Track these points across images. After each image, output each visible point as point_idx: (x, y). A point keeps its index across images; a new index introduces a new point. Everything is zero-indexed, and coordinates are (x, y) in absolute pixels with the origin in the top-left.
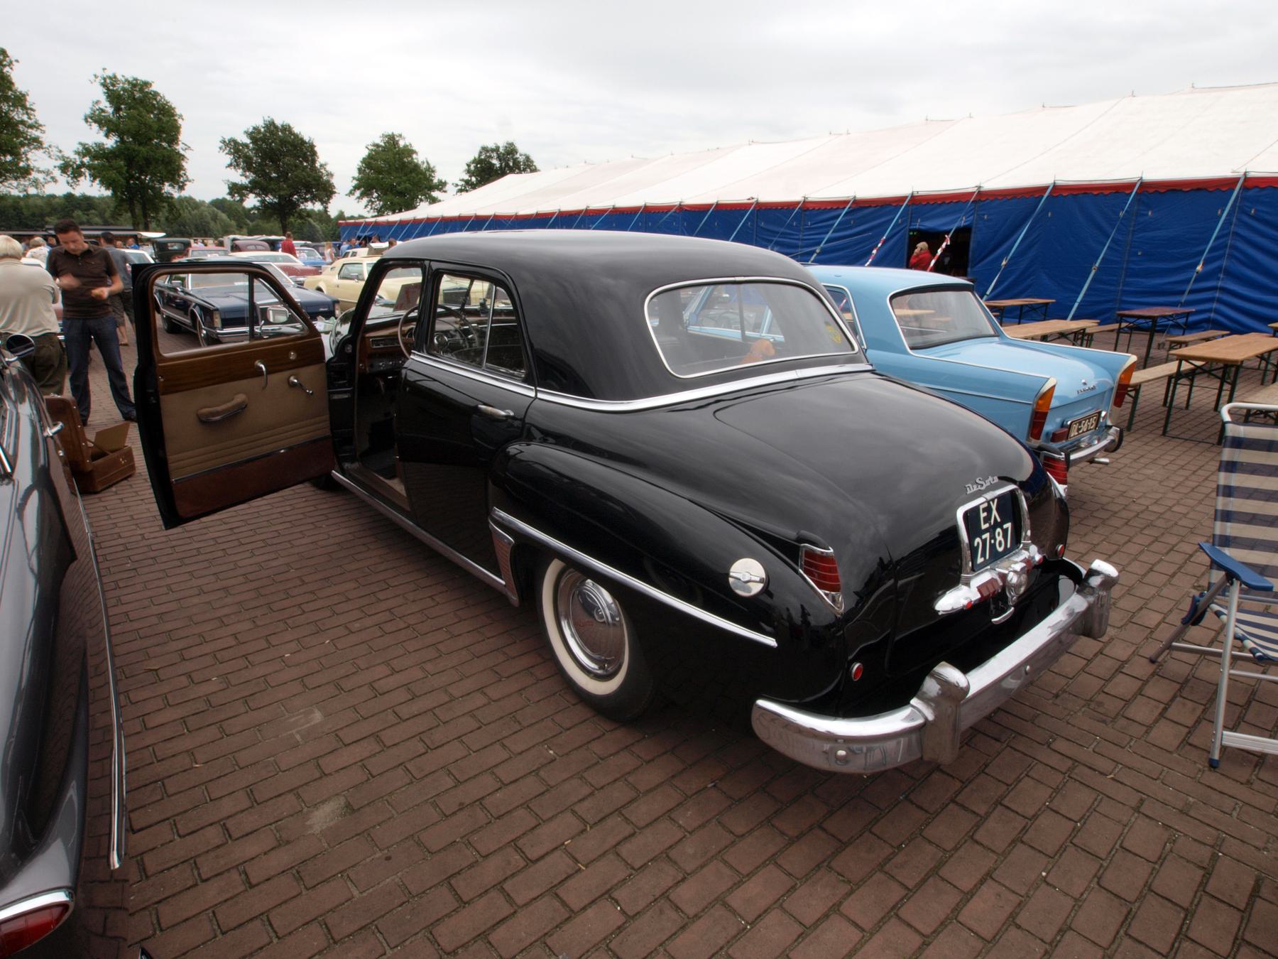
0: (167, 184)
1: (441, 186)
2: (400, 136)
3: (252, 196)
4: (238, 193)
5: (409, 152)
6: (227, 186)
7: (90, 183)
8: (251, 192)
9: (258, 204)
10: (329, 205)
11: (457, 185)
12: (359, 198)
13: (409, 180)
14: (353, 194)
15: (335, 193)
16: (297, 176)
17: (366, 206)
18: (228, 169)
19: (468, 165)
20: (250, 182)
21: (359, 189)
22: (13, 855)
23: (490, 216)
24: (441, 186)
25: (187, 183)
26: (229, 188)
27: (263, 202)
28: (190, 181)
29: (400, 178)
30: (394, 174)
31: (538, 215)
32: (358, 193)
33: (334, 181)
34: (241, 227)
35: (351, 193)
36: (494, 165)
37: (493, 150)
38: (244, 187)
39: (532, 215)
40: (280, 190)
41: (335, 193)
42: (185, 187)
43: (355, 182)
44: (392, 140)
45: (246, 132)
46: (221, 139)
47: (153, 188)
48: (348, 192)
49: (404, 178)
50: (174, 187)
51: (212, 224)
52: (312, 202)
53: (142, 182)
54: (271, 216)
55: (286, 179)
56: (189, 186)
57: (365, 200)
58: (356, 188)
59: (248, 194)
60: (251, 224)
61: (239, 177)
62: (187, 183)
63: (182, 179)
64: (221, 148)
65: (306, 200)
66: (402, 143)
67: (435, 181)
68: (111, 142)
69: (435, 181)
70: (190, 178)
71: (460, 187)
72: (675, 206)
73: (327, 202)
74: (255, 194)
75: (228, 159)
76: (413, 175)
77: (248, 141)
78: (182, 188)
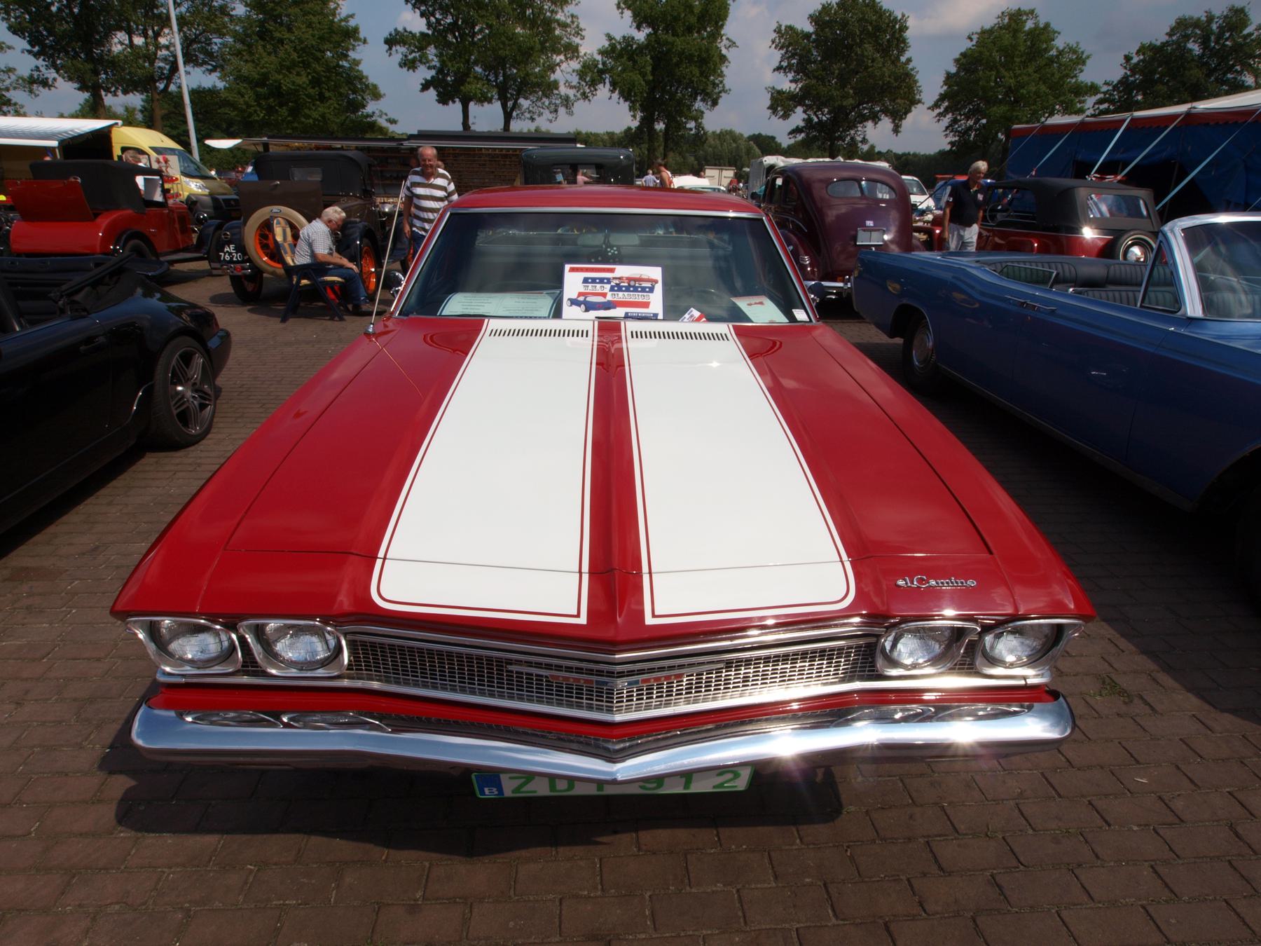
2: (1032, 12)
5: (1043, 34)
7: (609, 94)
12: (940, 115)
15: (919, 101)
17: (947, 128)
18: (776, 73)
19: (1128, 58)
26: (772, 98)
29: (1029, 75)
35: (936, 105)
36: (1191, 50)
37: (1196, 24)
41: (919, 101)
44: (1015, 19)
45: (811, 17)
46: (775, 26)
48: (931, 103)
58: (942, 98)
59: (796, 107)
61: (786, 84)
64: (773, 42)
66: (1029, 25)
68: (641, 36)
70: (727, 87)
73: (901, 119)
75: (776, 56)
77: (809, 28)
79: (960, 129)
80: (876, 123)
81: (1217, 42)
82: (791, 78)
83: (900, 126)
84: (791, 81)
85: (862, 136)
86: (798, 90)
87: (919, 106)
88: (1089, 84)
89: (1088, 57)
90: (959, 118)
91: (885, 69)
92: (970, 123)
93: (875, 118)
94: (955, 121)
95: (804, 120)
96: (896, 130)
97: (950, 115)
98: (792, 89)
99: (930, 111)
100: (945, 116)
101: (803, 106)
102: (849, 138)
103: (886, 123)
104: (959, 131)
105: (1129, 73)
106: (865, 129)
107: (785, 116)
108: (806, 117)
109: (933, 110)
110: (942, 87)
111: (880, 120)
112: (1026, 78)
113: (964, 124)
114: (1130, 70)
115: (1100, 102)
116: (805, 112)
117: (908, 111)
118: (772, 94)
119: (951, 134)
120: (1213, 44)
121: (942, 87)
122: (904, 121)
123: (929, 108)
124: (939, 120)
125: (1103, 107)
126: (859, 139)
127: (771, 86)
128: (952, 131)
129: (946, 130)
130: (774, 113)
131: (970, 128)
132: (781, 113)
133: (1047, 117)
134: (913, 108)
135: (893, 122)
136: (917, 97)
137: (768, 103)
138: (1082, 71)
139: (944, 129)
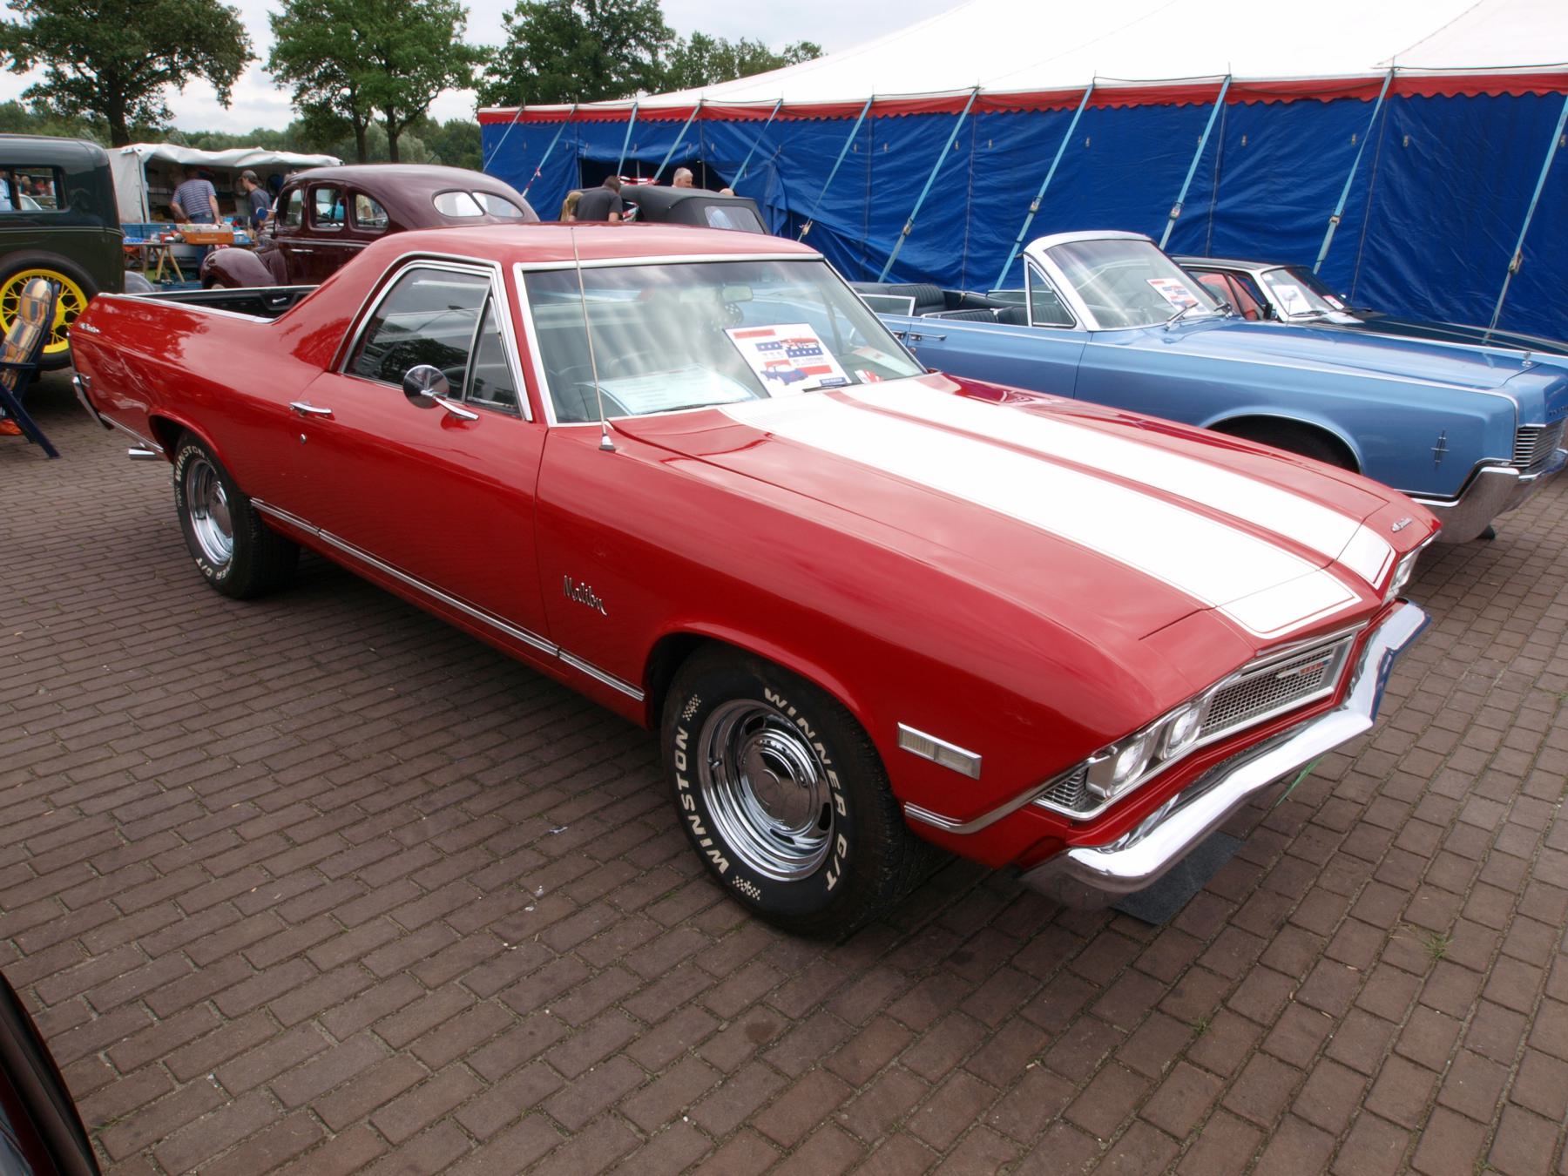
12: (278, 78)
15: (252, 57)
17: (295, 99)
19: (508, 19)
27: (58, 76)
35: (273, 65)
36: (578, 17)
40: (123, 42)
41: (252, 57)
65: (161, 77)
73: (228, 83)
80: (181, 87)
81: (603, 9)
83: (229, 93)
85: (162, 107)
88: (478, 49)
89: (467, 11)
90: (307, 84)
93: (174, 75)
94: (303, 89)
95: (47, 74)
96: (224, 98)
97: (293, 81)
102: (137, 108)
103: (200, 86)
105: (513, 37)
106: (162, 95)
107: (20, 67)
108: (50, 69)
113: (316, 97)
114: (514, 33)
117: (236, 71)
120: (599, 10)
122: (231, 87)
124: (280, 87)
126: (157, 110)
129: (294, 103)
132: (12, 62)
133: (437, 91)
135: (217, 86)
136: (248, 49)
138: (464, 29)
139: (291, 100)
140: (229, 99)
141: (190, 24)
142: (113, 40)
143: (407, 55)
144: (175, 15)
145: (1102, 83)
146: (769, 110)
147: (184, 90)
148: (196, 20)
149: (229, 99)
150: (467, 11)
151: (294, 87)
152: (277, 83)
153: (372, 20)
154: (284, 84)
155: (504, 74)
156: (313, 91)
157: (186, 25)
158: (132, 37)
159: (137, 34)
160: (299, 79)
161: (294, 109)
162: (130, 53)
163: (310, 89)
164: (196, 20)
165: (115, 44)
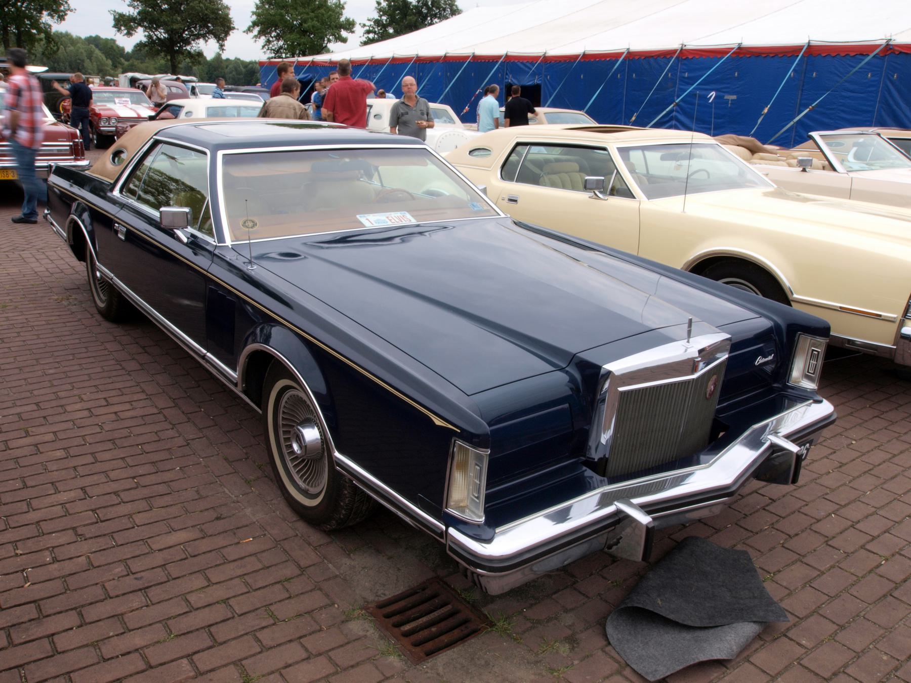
0: (45, 13)
1: (349, 26)
3: (140, 30)
4: (125, 26)
6: (112, 17)
8: (139, 25)
9: (144, 40)
10: (226, 43)
11: (364, 25)
12: (256, 37)
13: (316, 17)
14: (252, 31)
15: (234, 28)
16: (193, 8)
17: (263, 47)
20: (139, 13)
21: (258, 26)
22: (615, 623)
23: (500, 57)
24: (349, 26)
25: (69, 12)
26: (115, 19)
27: (150, 37)
28: (71, 11)
29: (308, 14)
30: (301, 10)
31: (585, 56)
32: (256, 30)
33: (232, 15)
34: (116, 67)
35: (249, 30)
38: (131, 19)
39: (575, 57)
40: (173, 22)
41: (234, 28)
42: (66, 17)
43: (254, 18)
47: (30, 18)
48: (246, 28)
49: (312, 14)
50: (52, 17)
51: (87, 61)
52: (204, 38)
53: (18, 9)
54: (158, 53)
55: (179, 12)
56: (69, 16)
57: (263, 39)
58: (255, 24)
59: (137, 28)
60: (126, 63)
62: (69, 12)
63: (62, 8)
65: (198, 37)
67: (342, 19)
69: (342, 19)
70: (72, 7)
71: (367, 28)
72: (878, 46)
73: (223, 40)
74: (146, 27)
76: (322, 11)
78: (61, 18)
79: (273, 48)
80: (206, 41)
82: (129, 3)
83: (224, 45)
84: (129, 6)
86: (136, 14)
87: (235, 31)
89: (345, 3)
90: (271, 39)
91: (201, 5)
92: (281, 43)
93: (204, 36)
94: (269, 42)
95: (145, 36)
98: (131, 14)
99: (245, 34)
100: (259, 38)
101: (142, 26)
104: (273, 50)
106: (199, 46)
107: (129, 34)
108: (147, 34)
109: (247, 33)
110: (251, 17)
111: (209, 38)
112: (305, 16)
115: (368, 32)
116: (145, 31)
117: (227, 34)
118: (114, 17)
119: (269, 51)
121: (251, 17)
123: (244, 32)
125: (371, 36)
127: (114, 10)
128: (268, 49)
130: (118, 31)
131: (281, 48)
132: (125, 32)
134: (231, 33)
137: (113, 23)
140: (224, 48)
141: (203, 14)
142: (169, 21)
143: (308, 26)
144: (196, 10)
145: (396, 56)
146: (326, 62)
147: (207, 43)
148: (206, 12)
149: (224, 48)
150: (345, 3)
151: (264, 41)
152: (255, 39)
153: (296, 9)
154: (257, 39)
155: (375, 32)
156: (275, 42)
157: (200, 14)
158: (177, 20)
159: (179, 18)
160: (266, 37)
161: (265, 52)
162: (174, 28)
163: (273, 42)
164: (206, 12)
165: (170, 23)
